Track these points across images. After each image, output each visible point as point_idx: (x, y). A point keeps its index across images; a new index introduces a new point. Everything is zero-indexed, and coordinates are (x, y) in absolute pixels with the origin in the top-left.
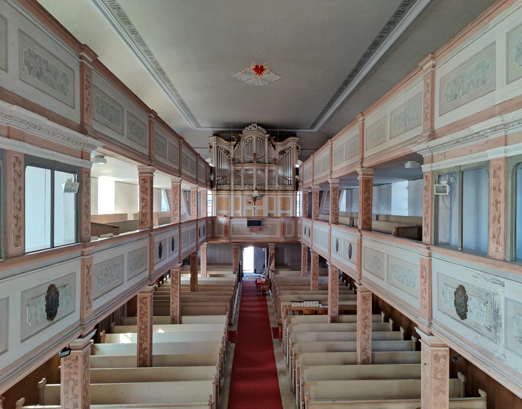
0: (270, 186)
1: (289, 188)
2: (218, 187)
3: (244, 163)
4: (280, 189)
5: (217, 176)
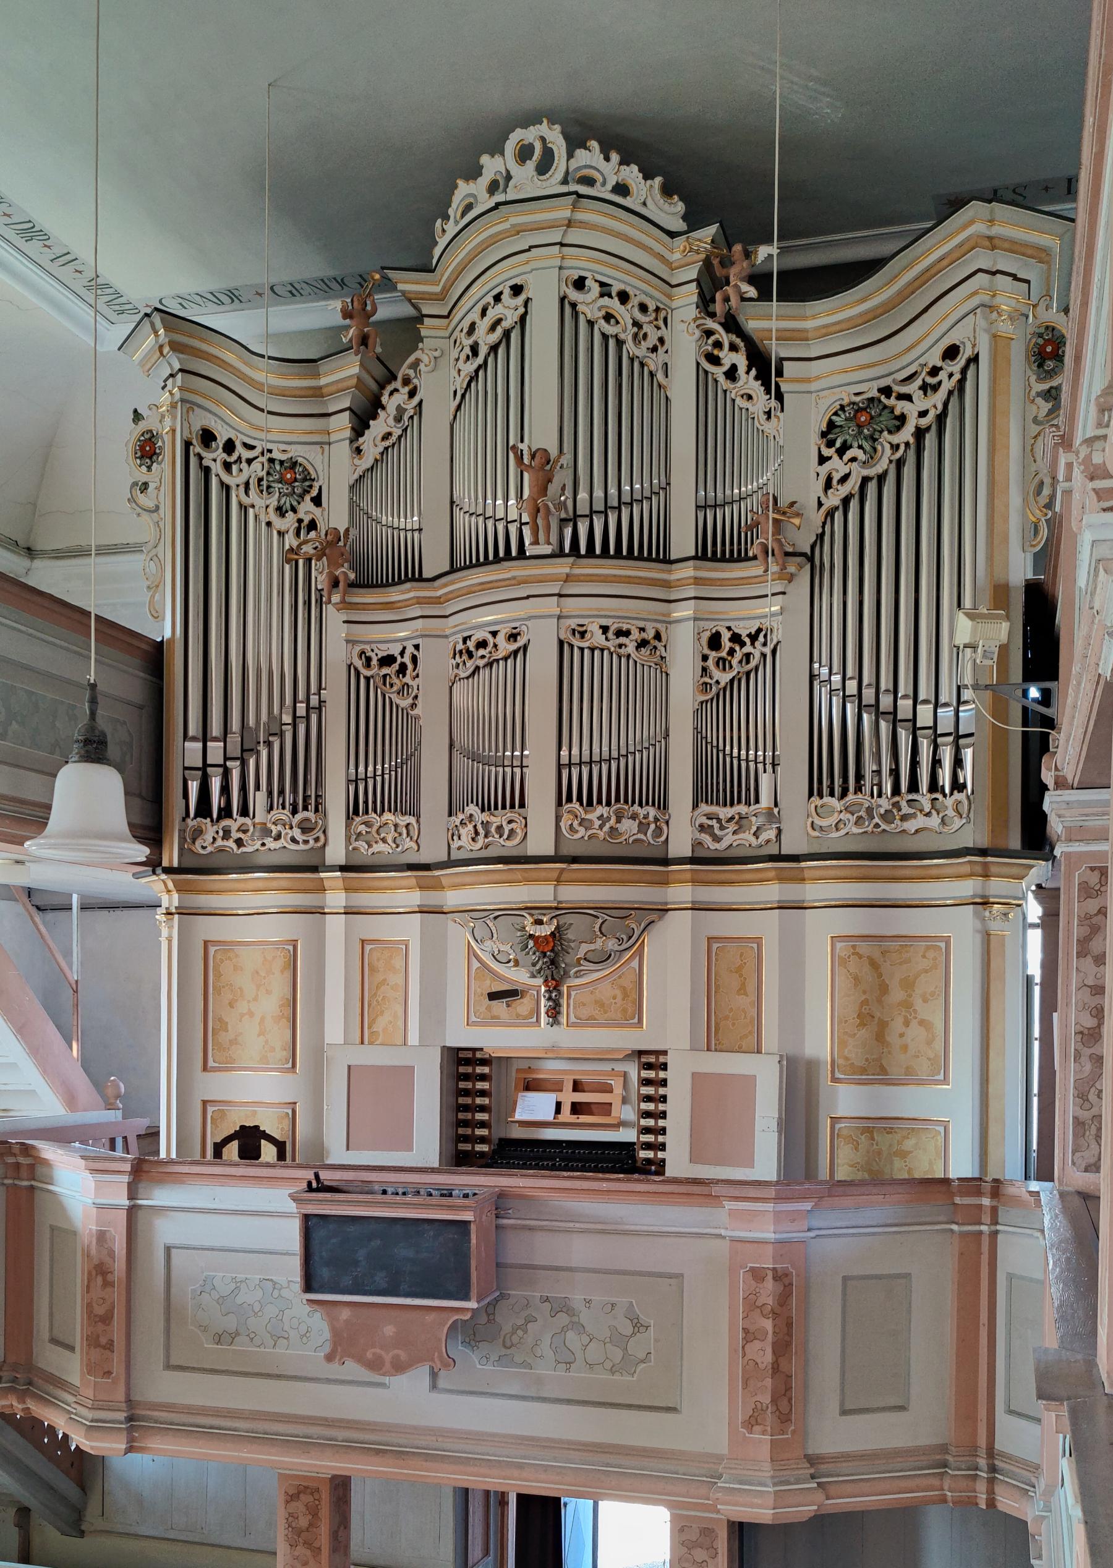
0: (725, 812)
1: (934, 821)
2: (198, 832)
3: (453, 570)
4: (835, 841)
5: (194, 729)
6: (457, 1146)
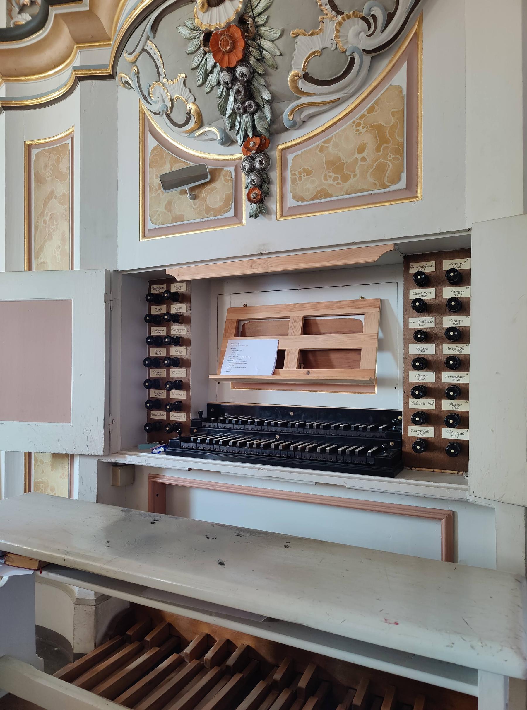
6: (149, 415)
